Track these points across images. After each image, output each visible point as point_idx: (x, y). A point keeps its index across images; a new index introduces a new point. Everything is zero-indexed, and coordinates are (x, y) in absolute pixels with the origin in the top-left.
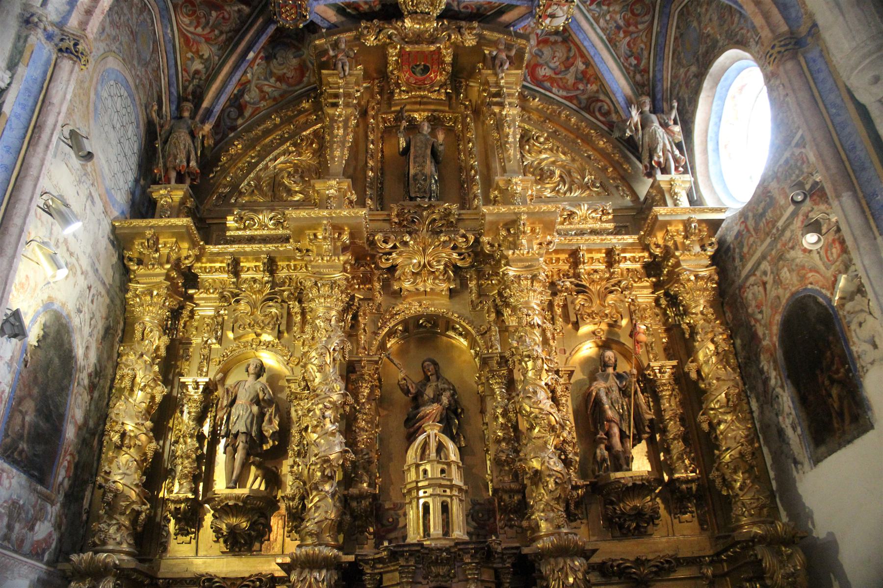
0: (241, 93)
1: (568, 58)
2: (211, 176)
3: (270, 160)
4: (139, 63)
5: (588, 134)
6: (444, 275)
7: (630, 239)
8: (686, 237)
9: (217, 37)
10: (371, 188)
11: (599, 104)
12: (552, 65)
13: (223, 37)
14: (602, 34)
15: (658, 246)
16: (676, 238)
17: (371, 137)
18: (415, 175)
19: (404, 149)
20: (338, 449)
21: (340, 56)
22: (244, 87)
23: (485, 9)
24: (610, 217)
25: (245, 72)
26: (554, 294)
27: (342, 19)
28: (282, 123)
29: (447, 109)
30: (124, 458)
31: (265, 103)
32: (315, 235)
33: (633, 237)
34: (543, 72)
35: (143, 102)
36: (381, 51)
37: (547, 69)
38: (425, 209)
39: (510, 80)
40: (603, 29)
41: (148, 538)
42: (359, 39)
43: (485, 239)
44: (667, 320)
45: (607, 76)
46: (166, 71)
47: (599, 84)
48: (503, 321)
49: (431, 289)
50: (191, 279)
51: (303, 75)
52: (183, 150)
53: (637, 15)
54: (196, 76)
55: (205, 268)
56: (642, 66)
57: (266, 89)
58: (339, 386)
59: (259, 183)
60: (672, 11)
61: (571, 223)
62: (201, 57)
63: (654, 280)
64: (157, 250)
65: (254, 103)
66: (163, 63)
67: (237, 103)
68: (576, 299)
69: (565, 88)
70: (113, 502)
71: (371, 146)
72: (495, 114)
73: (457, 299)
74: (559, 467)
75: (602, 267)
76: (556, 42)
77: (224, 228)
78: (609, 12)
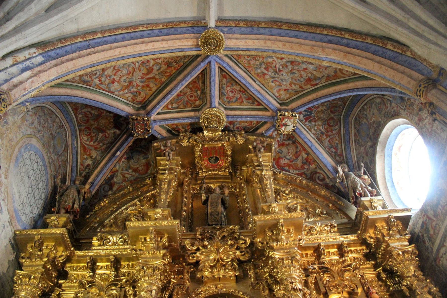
0: (112, 177)
1: (296, 152)
2: (87, 216)
3: (124, 209)
4: (53, 152)
5: (314, 188)
6: (231, 266)
7: (352, 237)
8: (389, 229)
9: (101, 147)
10: (184, 221)
11: (318, 175)
12: (288, 157)
13: (105, 146)
14: (314, 137)
15: (371, 238)
16: (382, 231)
18: (212, 212)
19: (204, 200)
21: (167, 150)
22: (113, 174)
23: (248, 128)
24: (336, 229)
25: (115, 166)
26: (307, 276)
27: (170, 135)
28: (133, 190)
29: (230, 181)
31: (125, 184)
32: (145, 239)
33: (354, 235)
34: (283, 162)
35: (53, 173)
36: (191, 149)
37: (286, 160)
38: (218, 230)
39: (265, 158)
40: (313, 134)
42: (179, 143)
44: (389, 288)
45: (320, 157)
46: (71, 164)
47: (316, 163)
48: (274, 295)
49: (223, 276)
51: (148, 169)
52: (72, 199)
53: (332, 126)
54: (88, 167)
55: (73, 267)
56: (339, 152)
57: (127, 175)
59: (116, 221)
60: (350, 121)
61: (312, 234)
62: (91, 157)
63: (373, 262)
64: (41, 250)
65: (119, 183)
66: (69, 159)
67: (109, 183)
68: (323, 277)
69: (297, 169)
71: (185, 199)
72: (258, 175)
75: (337, 257)
76: (289, 144)
78: (316, 125)
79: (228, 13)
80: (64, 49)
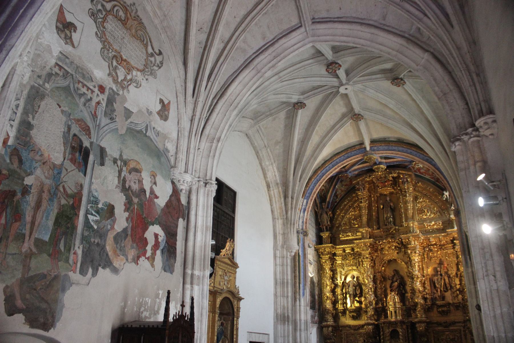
0: (336, 192)
17: (373, 204)
30: (328, 301)
34: (422, 171)
41: (336, 317)
43: (403, 241)
50: (335, 254)
52: (325, 219)
58: (371, 283)
67: (336, 196)
73: (399, 254)
74: (422, 301)
77: (340, 238)
79: (375, 136)
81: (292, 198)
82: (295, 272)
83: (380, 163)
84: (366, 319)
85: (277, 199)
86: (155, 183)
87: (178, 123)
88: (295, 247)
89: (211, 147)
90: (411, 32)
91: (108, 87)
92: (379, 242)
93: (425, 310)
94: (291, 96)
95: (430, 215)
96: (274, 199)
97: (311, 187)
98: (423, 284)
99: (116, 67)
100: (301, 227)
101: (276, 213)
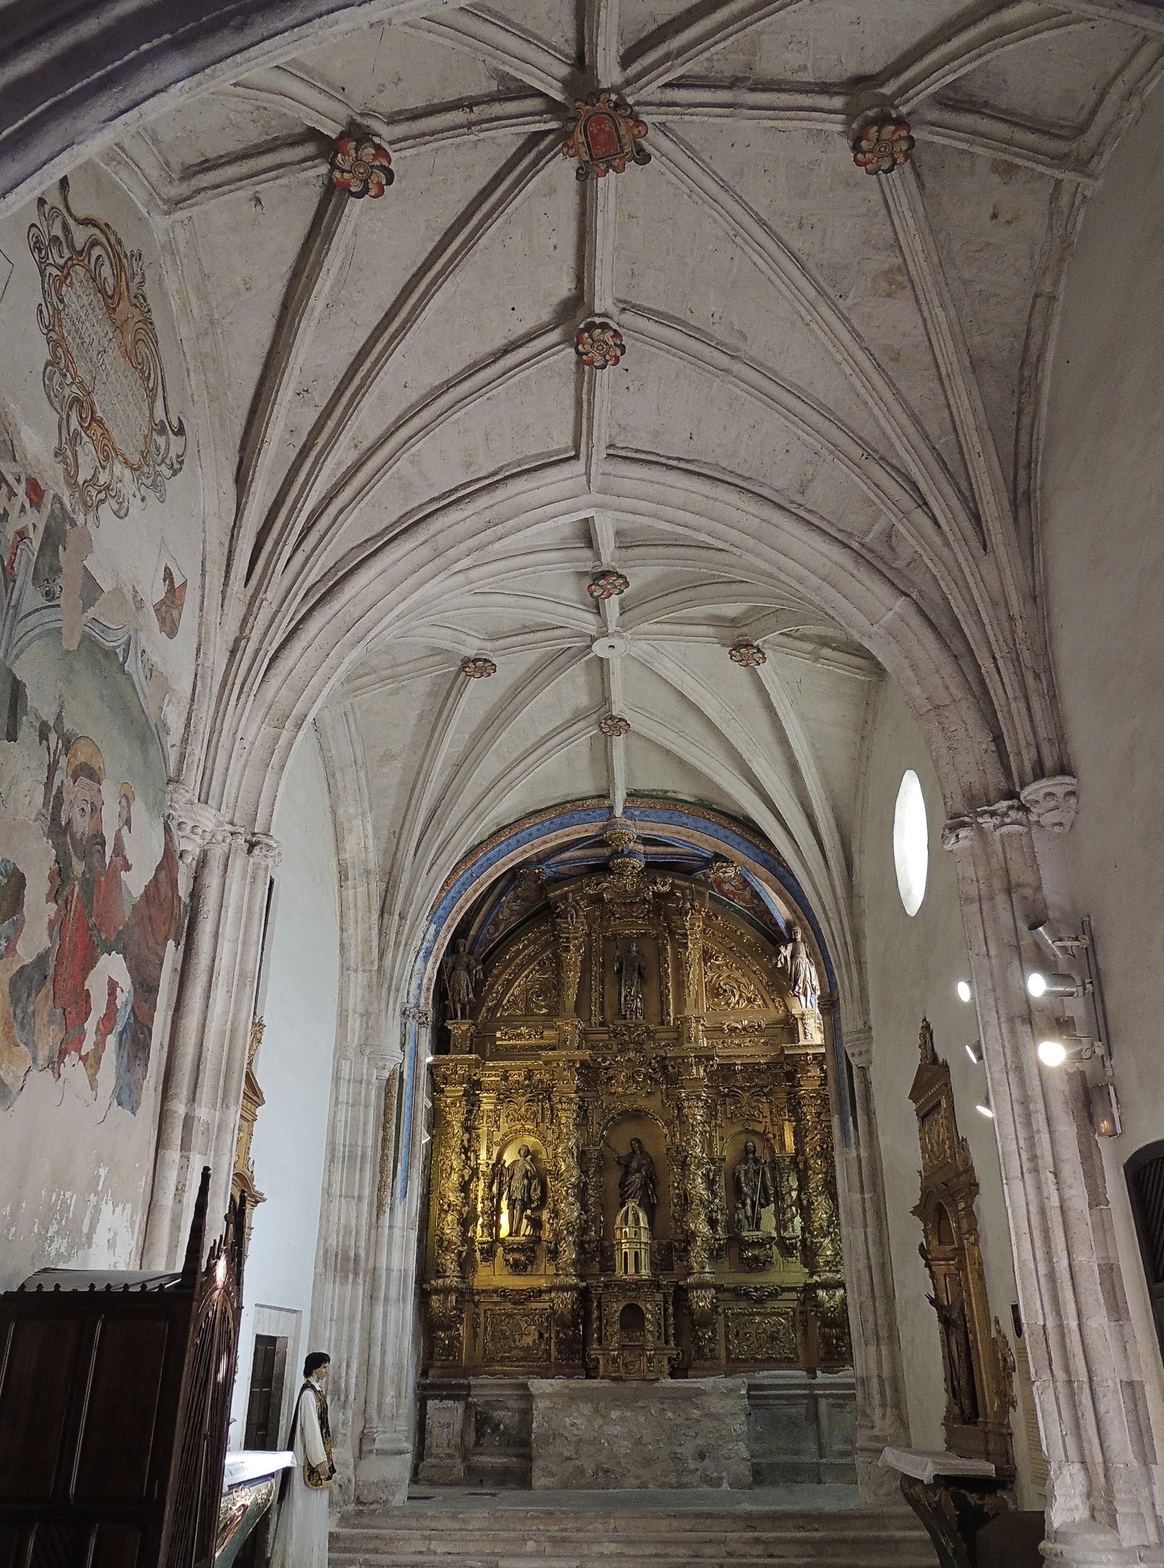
20: (576, 1214)
34: (726, 887)
41: (466, 1265)
50: (477, 1085)
70: (444, 1244)
74: (704, 1229)
80: (449, 897)
81: (402, 917)
82: (385, 1129)
83: (631, 854)
84: (551, 1270)
85: (360, 915)
86: (128, 822)
87: (198, 650)
88: (395, 1057)
89: (276, 739)
90: (867, 540)
91: (52, 492)
92: (604, 1060)
93: (711, 1253)
94: (464, 637)
95: (738, 1002)
96: (351, 912)
97: (452, 893)
98: (710, 1183)
99: (77, 434)
100: (412, 1001)
101: (353, 953)
